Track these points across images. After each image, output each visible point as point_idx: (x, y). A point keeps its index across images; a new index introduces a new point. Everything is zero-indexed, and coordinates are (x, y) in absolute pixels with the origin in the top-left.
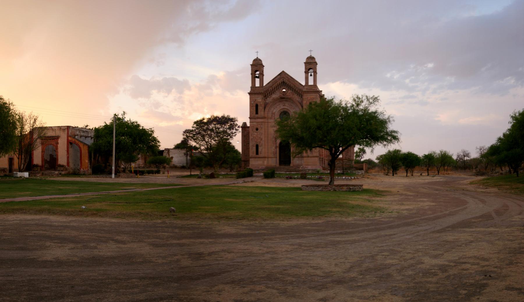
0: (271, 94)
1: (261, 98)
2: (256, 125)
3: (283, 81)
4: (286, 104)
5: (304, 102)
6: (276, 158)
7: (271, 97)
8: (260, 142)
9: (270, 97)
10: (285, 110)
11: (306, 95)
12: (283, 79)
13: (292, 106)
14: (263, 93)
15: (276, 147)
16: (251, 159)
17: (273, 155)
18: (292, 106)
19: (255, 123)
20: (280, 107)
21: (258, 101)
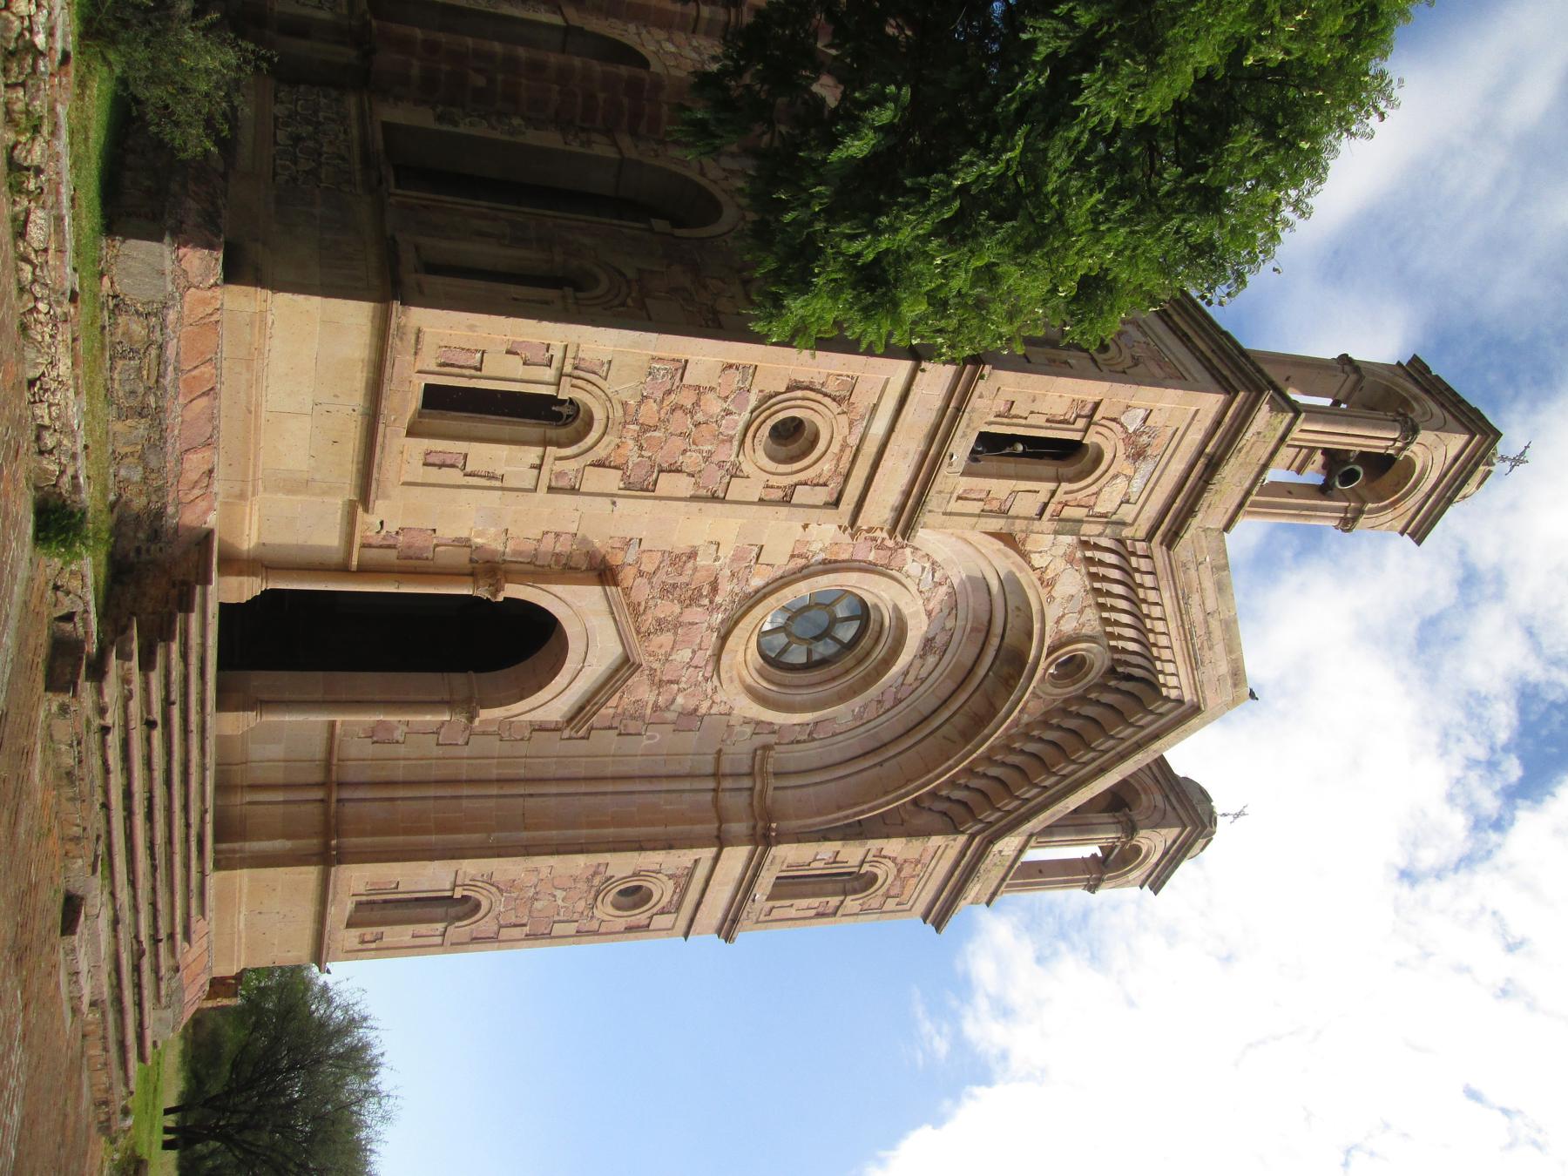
0: (1094, 577)
1: (1128, 512)
2: (853, 441)
3: (1167, 699)
4: (931, 660)
5: (895, 847)
6: (343, 570)
7: (1071, 561)
8: (600, 464)
9: (1079, 555)
10: (880, 652)
11: (952, 854)
12: (1180, 702)
13: (898, 702)
14: (1171, 540)
15: (491, 568)
16: (356, 315)
17: (392, 527)
18: (898, 702)
19: (879, 427)
20: (929, 614)
21: (1115, 477)
